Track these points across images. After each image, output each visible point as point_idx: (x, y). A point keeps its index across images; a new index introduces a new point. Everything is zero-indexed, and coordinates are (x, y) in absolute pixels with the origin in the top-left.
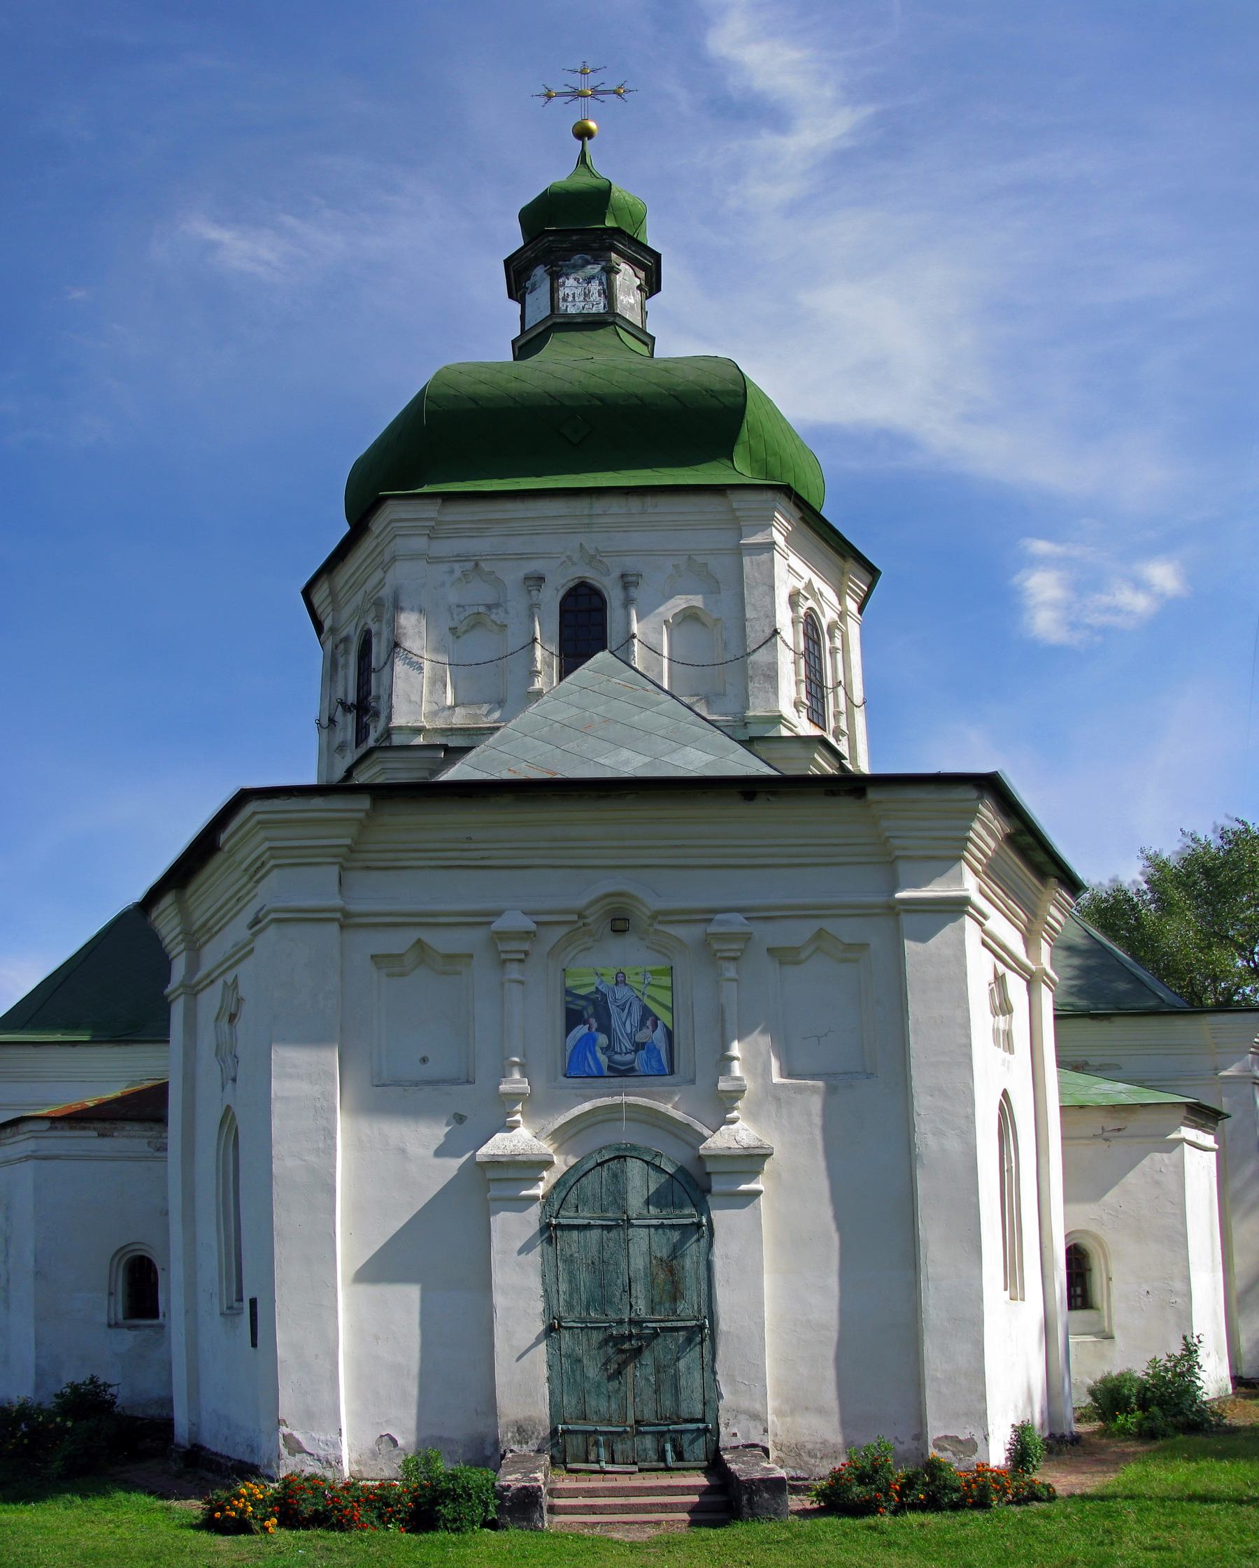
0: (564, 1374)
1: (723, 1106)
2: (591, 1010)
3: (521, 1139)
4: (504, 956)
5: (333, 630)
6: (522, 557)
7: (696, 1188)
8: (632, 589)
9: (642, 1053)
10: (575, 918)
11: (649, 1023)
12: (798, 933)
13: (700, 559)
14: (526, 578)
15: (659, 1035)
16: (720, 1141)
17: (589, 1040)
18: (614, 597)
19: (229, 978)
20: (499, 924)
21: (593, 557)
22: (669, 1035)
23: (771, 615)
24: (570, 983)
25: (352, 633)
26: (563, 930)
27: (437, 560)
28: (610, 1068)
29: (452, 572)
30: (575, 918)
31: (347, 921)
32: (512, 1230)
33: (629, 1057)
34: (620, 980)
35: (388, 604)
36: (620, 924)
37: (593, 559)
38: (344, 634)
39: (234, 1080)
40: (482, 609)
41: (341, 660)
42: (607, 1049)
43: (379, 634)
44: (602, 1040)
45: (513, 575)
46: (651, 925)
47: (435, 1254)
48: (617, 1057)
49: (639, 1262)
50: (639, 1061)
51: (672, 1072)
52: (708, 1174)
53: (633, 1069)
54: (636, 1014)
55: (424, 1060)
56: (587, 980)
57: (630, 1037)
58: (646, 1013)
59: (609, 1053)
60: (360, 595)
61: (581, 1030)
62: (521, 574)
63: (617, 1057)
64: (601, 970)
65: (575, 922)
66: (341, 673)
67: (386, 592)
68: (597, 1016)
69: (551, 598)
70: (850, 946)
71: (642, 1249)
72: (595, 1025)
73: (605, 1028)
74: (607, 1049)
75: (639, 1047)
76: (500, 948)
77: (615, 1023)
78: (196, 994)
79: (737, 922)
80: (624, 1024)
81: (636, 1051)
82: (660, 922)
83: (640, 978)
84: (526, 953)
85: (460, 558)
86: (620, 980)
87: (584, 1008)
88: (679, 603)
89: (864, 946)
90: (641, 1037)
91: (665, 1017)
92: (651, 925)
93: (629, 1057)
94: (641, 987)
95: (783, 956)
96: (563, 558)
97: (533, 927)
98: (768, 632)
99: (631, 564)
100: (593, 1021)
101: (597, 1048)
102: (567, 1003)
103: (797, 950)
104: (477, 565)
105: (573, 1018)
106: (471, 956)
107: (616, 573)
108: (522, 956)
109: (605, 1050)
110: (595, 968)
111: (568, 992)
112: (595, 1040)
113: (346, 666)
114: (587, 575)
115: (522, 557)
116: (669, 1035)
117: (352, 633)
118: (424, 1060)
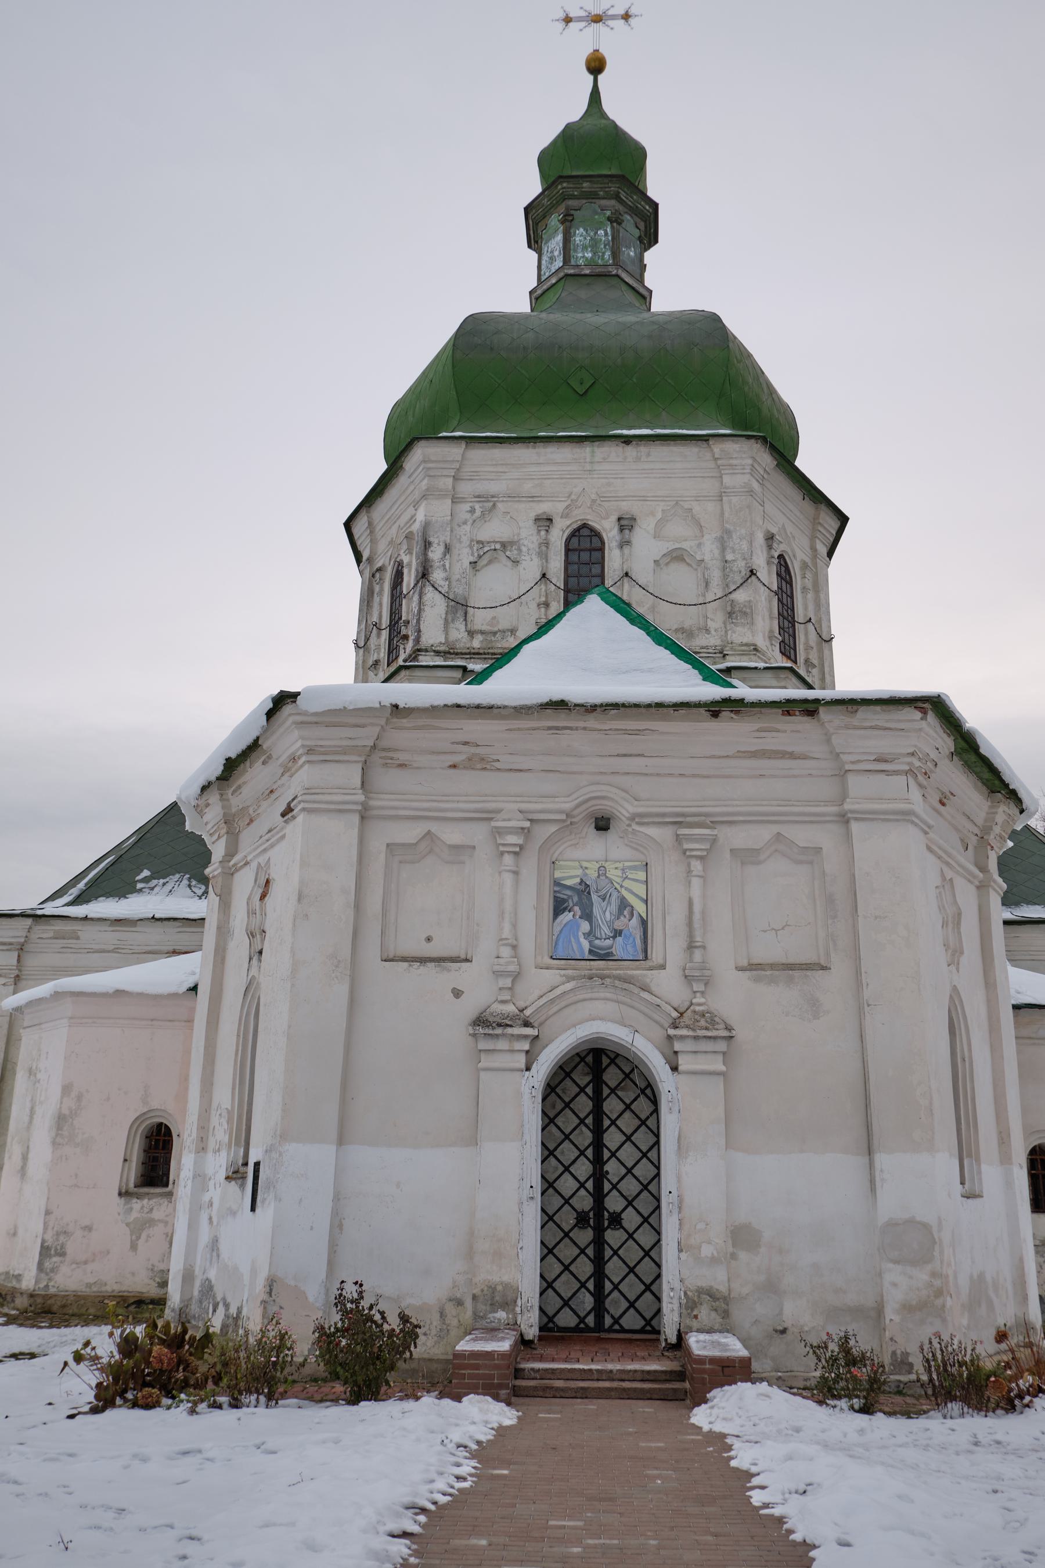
2: (576, 899)
4: (502, 848)
5: (370, 560)
6: (532, 498)
8: (627, 532)
9: (619, 939)
10: (564, 817)
11: (626, 913)
13: (686, 505)
14: (537, 520)
15: (635, 921)
17: (572, 926)
19: (262, 860)
21: (594, 501)
22: (644, 923)
23: (748, 557)
24: (558, 874)
25: (387, 563)
26: (553, 828)
28: (590, 951)
29: (472, 511)
30: (564, 817)
33: (608, 942)
34: (602, 871)
35: (417, 538)
36: (602, 824)
38: (379, 565)
39: (260, 952)
40: (498, 546)
41: (377, 588)
43: (409, 565)
44: (585, 926)
46: (629, 825)
48: (597, 942)
50: (619, 947)
51: (646, 958)
52: (676, 1053)
53: (611, 954)
54: (614, 907)
55: (429, 939)
56: (573, 873)
57: (609, 924)
58: (623, 904)
59: (591, 938)
60: (394, 529)
61: (566, 917)
62: (533, 515)
63: (597, 942)
64: (585, 864)
65: (564, 821)
66: (376, 599)
67: (416, 527)
68: (579, 903)
69: (558, 537)
70: (805, 849)
72: (579, 913)
73: (588, 916)
75: (617, 933)
76: (499, 841)
77: (597, 911)
78: (232, 874)
80: (604, 912)
81: (614, 937)
82: (638, 823)
83: (619, 873)
84: (521, 847)
85: (480, 497)
86: (602, 871)
87: (570, 897)
89: (818, 850)
90: (618, 925)
91: (640, 908)
92: (629, 825)
93: (608, 942)
94: (619, 880)
96: (569, 502)
97: (527, 824)
98: (745, 573)
99: (627, 507)
100: (577, 908)
101: (580, 934)
102: (555, 892)
103: (757, 851)
104: (494, 505)
105: (559, 907)
106: (474, 847)
107: (614, 518)
108: (517, 849)
109: (587, 935)
111: (557, 883)
112: (578, 926)
113: (382, 590)
114: (588, 517)
116: (644, 923)
117: (387, 563)
118: (429, 939)
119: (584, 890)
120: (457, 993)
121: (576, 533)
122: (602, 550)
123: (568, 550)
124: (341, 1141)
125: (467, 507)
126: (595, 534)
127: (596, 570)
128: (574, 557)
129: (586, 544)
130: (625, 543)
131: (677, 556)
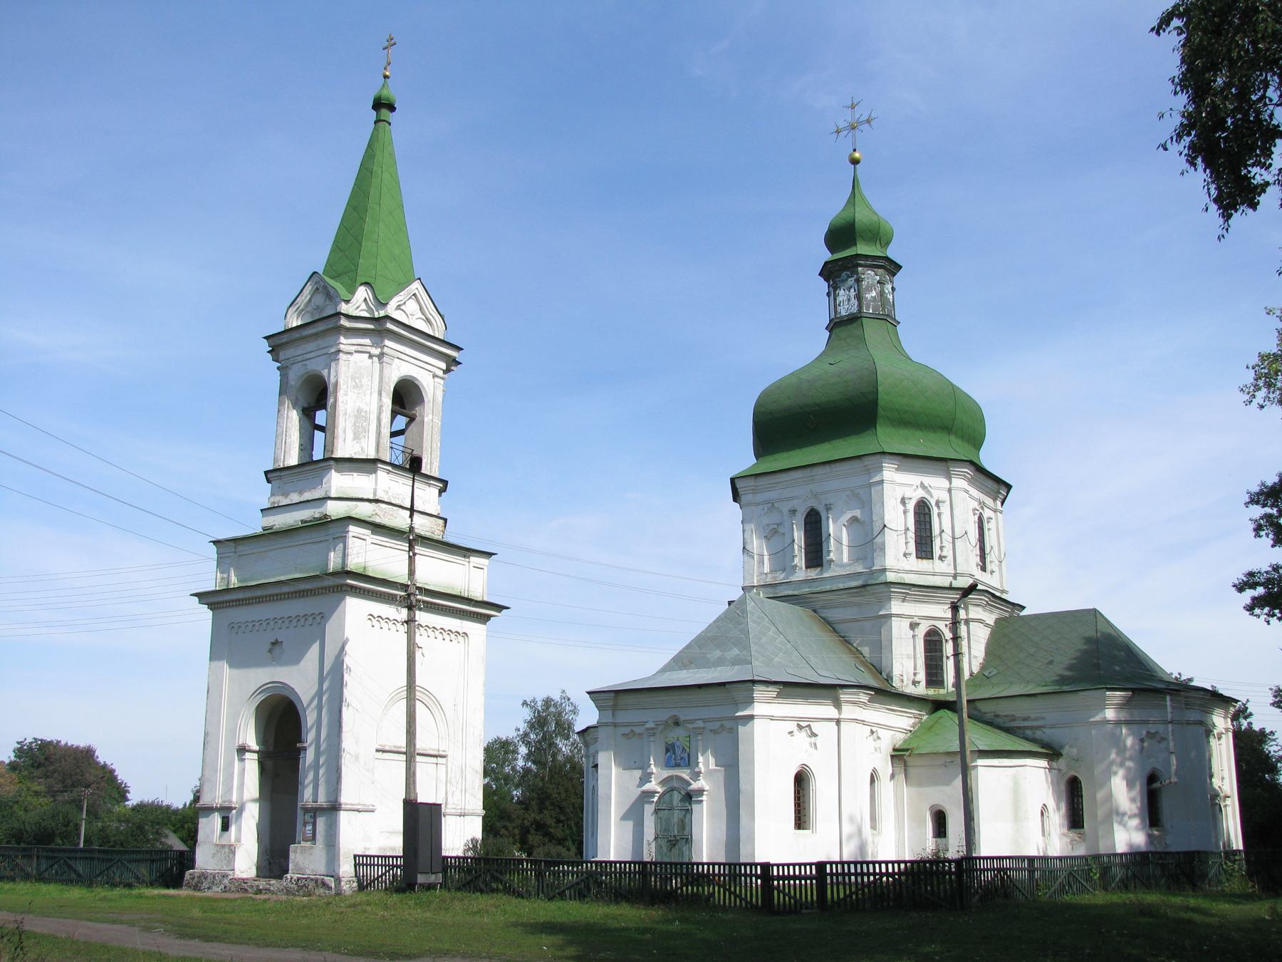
0: (659, 848)
1: (696, 775)
3: (653, 785)
7: (690, 797)
12: (716, 725)
16: (695, 786)
20: (648, 726)
27: (758, 504)
31: (615, 725)
32: (649, 809)
36: (677, 723)
37: (816, 496)
45: (785, 508)
47: (634, 813)
49: (676, 820)
71: (677, 815)
79: (700, 724)
80: (678, 752)
85: (767, 502)
88: (848, 515)
95: (714, 732)
105: (667, 750)
119: (673, 746)
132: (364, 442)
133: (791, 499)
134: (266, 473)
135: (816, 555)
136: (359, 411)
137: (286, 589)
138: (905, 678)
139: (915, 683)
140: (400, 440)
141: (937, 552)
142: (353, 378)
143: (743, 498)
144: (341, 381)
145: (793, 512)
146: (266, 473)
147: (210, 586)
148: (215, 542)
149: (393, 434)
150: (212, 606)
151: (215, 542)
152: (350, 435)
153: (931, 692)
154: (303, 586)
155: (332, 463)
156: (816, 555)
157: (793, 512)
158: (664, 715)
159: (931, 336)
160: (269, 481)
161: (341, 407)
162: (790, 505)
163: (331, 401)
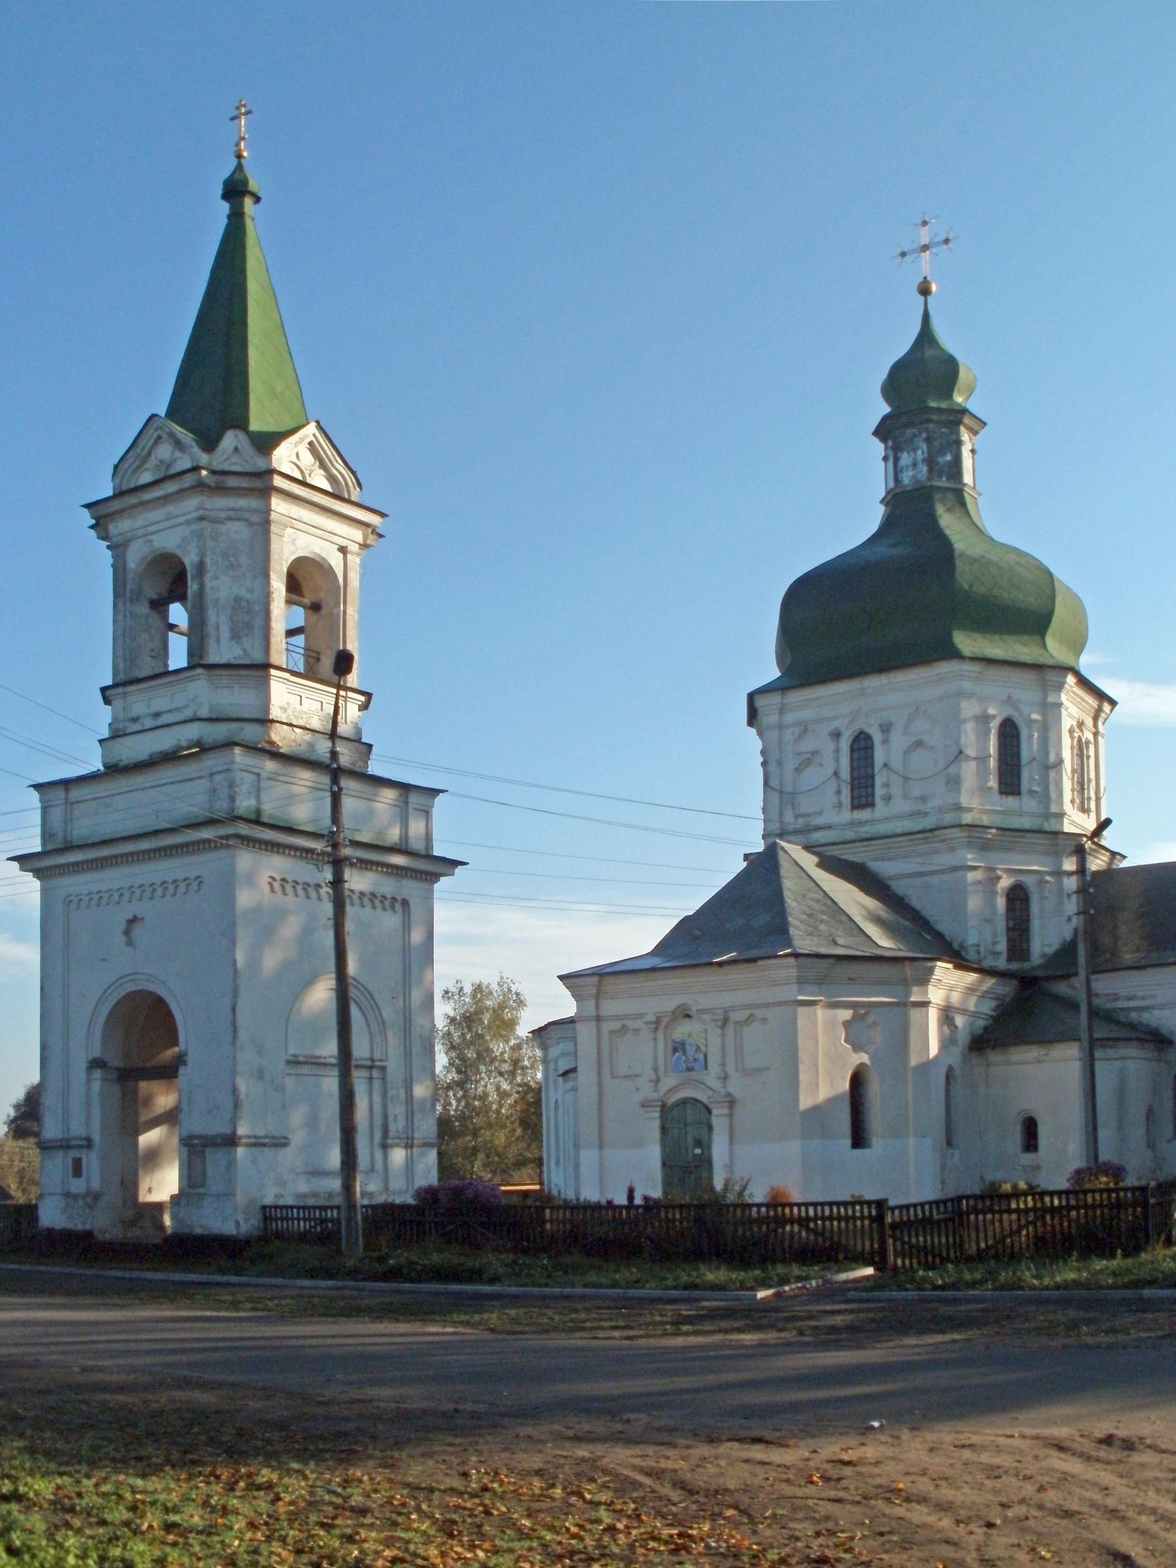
6: (829, 719)
17: (679, 1059)
18: (877, 738)
34: (690, 1035)
36: (688, 1016)
42: (686, 1062)
50: (696, 1065)
69: (845, 744)
73: (685, 1053)
74: (686, 1062)
75: (695, 1060)
80: (690, 1051)
86: (690, 1035)
105: (675, 1050)
110: (682, 1031)
115: (829, 719)
116: (705, 1056)
120: (638, 1089)
121: (856, 739)
122: (872, 748)
123: (852, 750)
124: (601, 1147)
125: (789, 731)
126: (868, 738)
127: (856, 774)
128: (856, 756)
129: (863, 744)
130: (885, 742)
131: (919, 744)
132: (247, 643)
133: (836, 718)
134: (104, 690)
135: (862, 792)
136: (238, 599)
137: (145, 845)
138: (982, 949)
139: (996, 954)
140: (300, 640)
141: (1025, 786)
142: (225, 556)
143: (769, 718)
144: (208, 561)
145: (836, 735)
146: (104, 690)
147: (35, 846)
148: (38, 787)
149: (290, 633)
150: (39, 873)
151: (38, 787)
152: (225, 633)
153: (1014, 966)
154: (169, 840)
155: (199, 671)
156: (862, 792)
157: (836, 735)
158: (670, 1004)
159: (1006, 506)
160: (107, 701)
161: (210, 595)
162: (832, 726)
163: (192, 587)
